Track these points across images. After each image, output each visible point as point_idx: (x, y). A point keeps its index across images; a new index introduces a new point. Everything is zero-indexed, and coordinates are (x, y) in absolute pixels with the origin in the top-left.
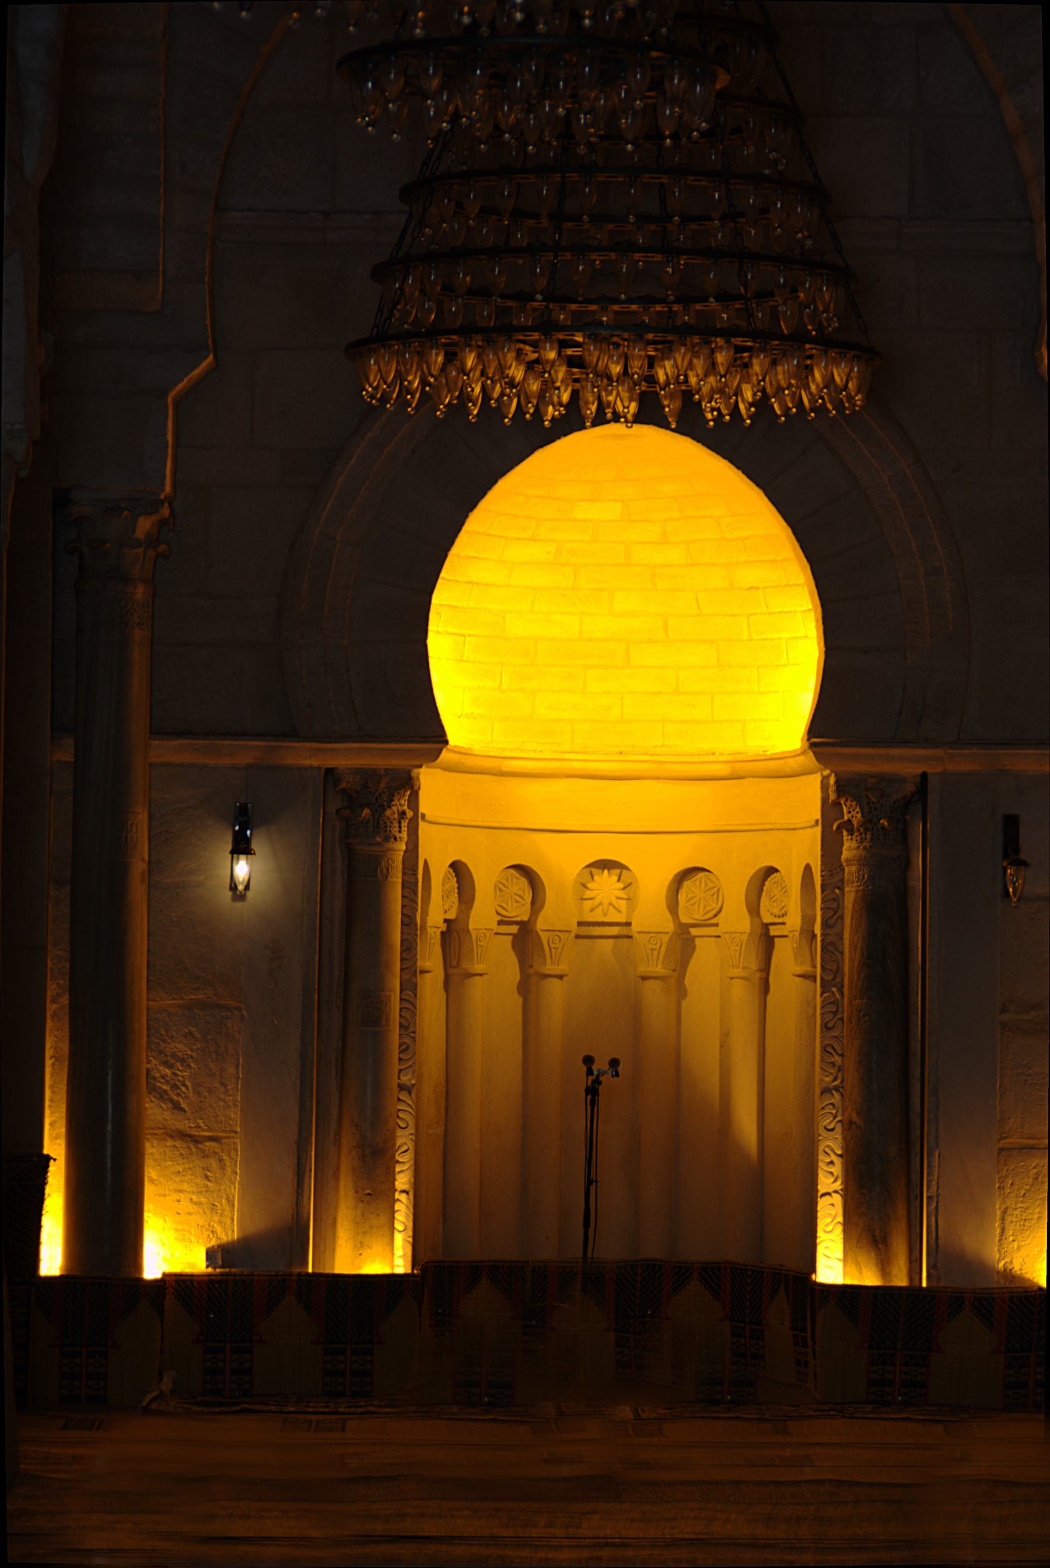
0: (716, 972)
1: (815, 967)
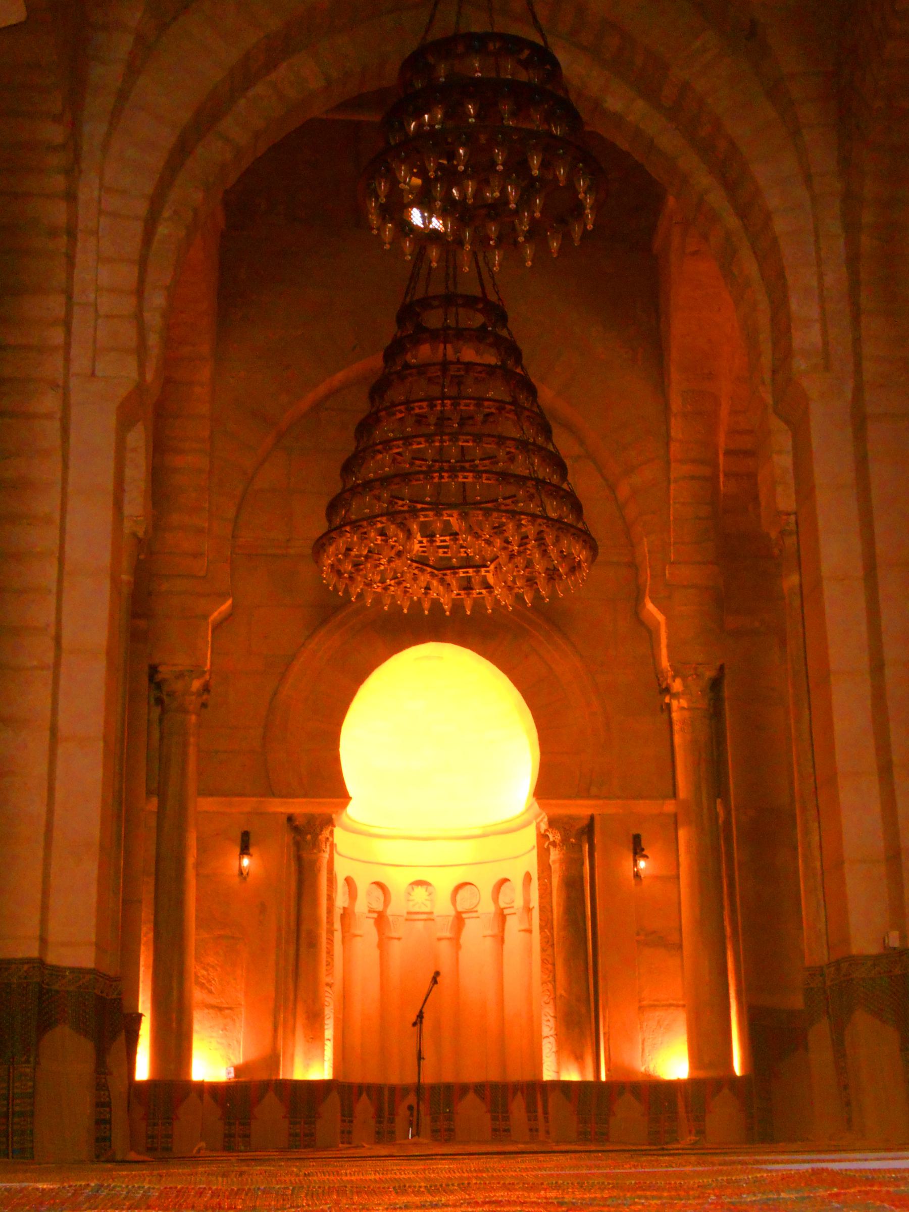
0: (476, 932)
1: (530, 924)
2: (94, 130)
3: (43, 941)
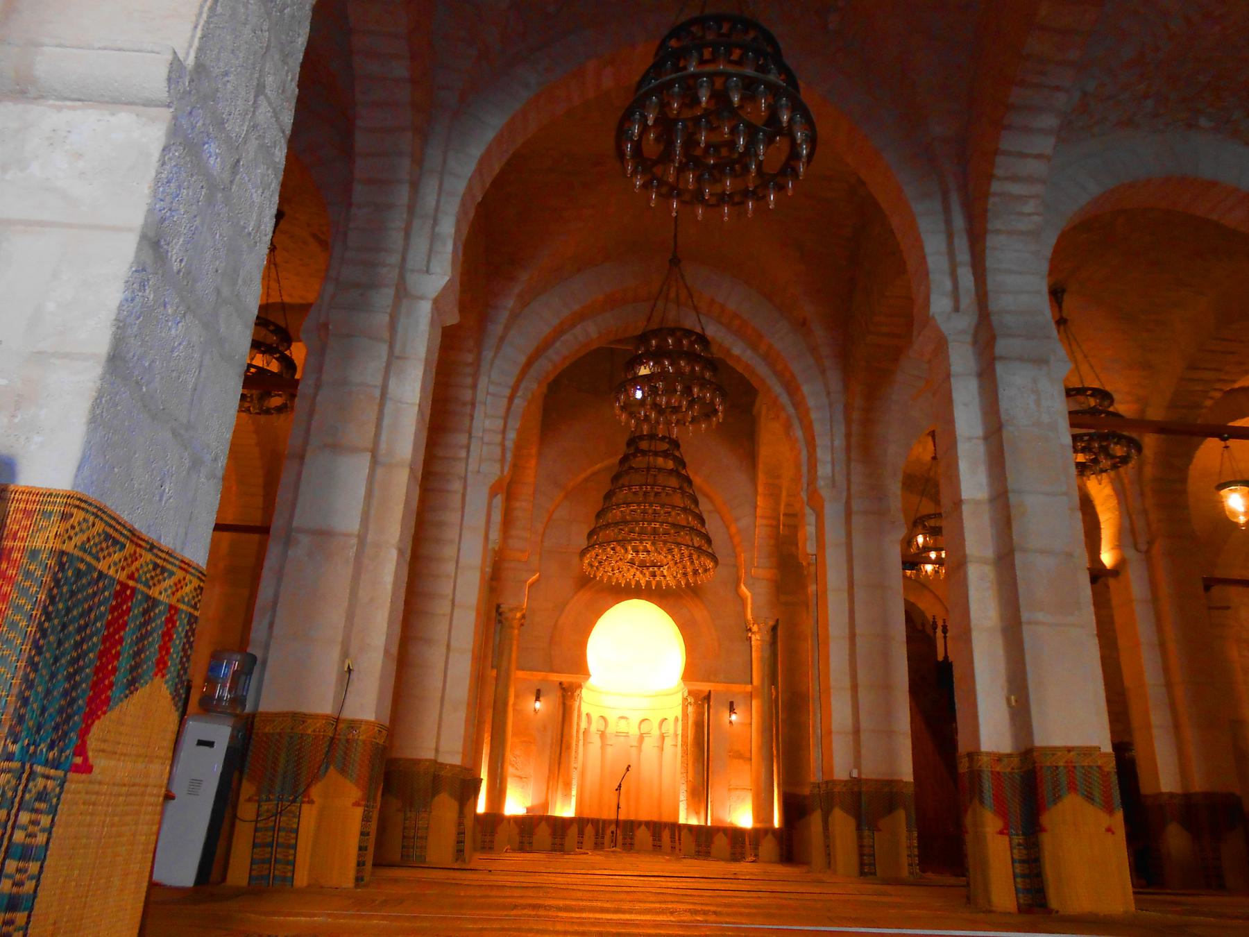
0: (650, 744)
2: (488, 355)
3: (437, 750)
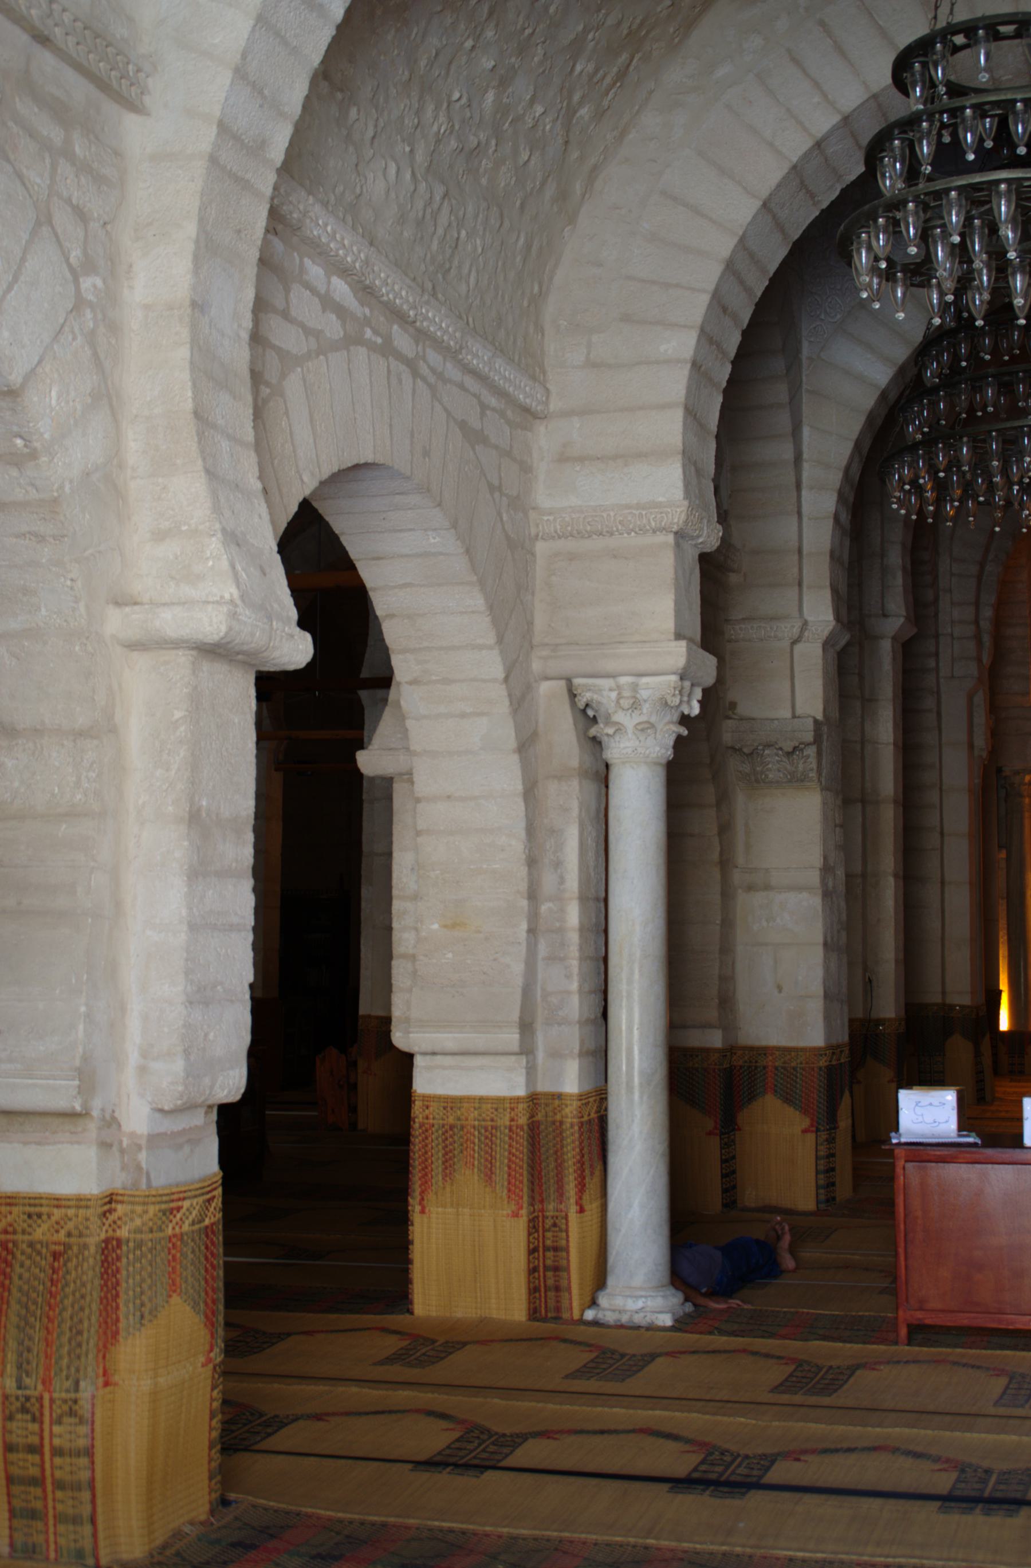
3: (944, 993)
